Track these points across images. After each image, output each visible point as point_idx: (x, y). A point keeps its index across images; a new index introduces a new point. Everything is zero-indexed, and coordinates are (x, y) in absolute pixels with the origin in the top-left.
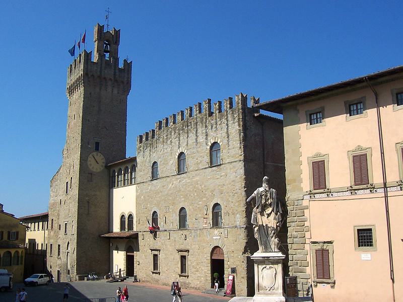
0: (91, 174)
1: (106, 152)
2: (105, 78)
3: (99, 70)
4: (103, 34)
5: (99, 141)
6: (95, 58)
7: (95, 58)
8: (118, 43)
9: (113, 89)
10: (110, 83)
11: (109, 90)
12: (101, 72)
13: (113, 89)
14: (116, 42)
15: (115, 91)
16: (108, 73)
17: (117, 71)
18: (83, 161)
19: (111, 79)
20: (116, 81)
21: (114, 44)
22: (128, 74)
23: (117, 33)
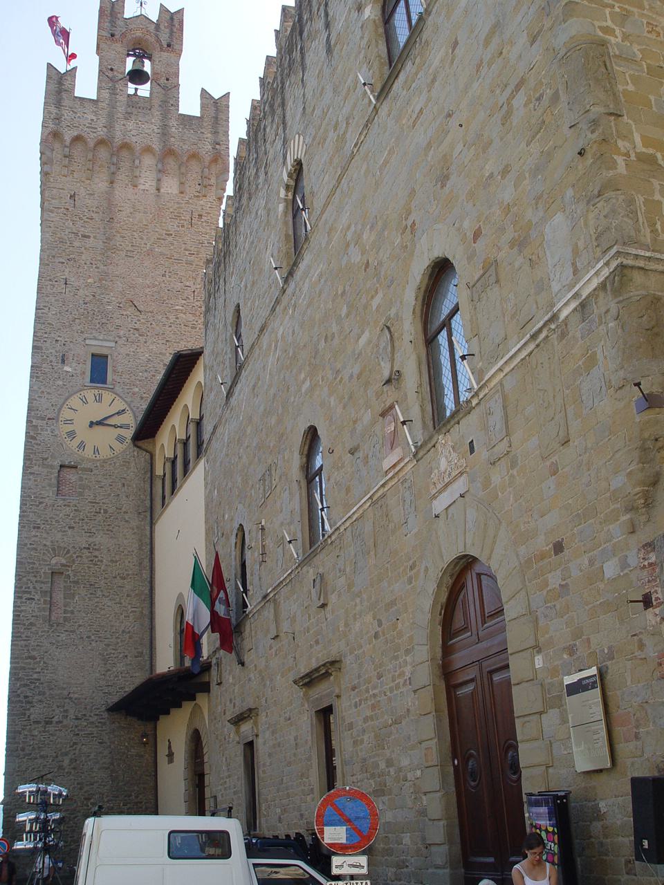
0: (76, 467)
1: (137, 390)
2: (126, 146)
3: (103, 121)
4: (120, 23)
5: (105, 352)
6: (87, 86)
7: (87, 86)
8: (176, 47)
9: (159, 180)
10: (148, 161)
11: (147, 181)
12: (110, 126)
13: (159, 180)
14: (169, 45)
15: (170, 186)
16: (141, 131)
17: (173, 123)
18: (40, 422)
19: (148, 150)
20: (169, 152)
21: (162, 50)
22: (216, 133)
23: (173, 22)
